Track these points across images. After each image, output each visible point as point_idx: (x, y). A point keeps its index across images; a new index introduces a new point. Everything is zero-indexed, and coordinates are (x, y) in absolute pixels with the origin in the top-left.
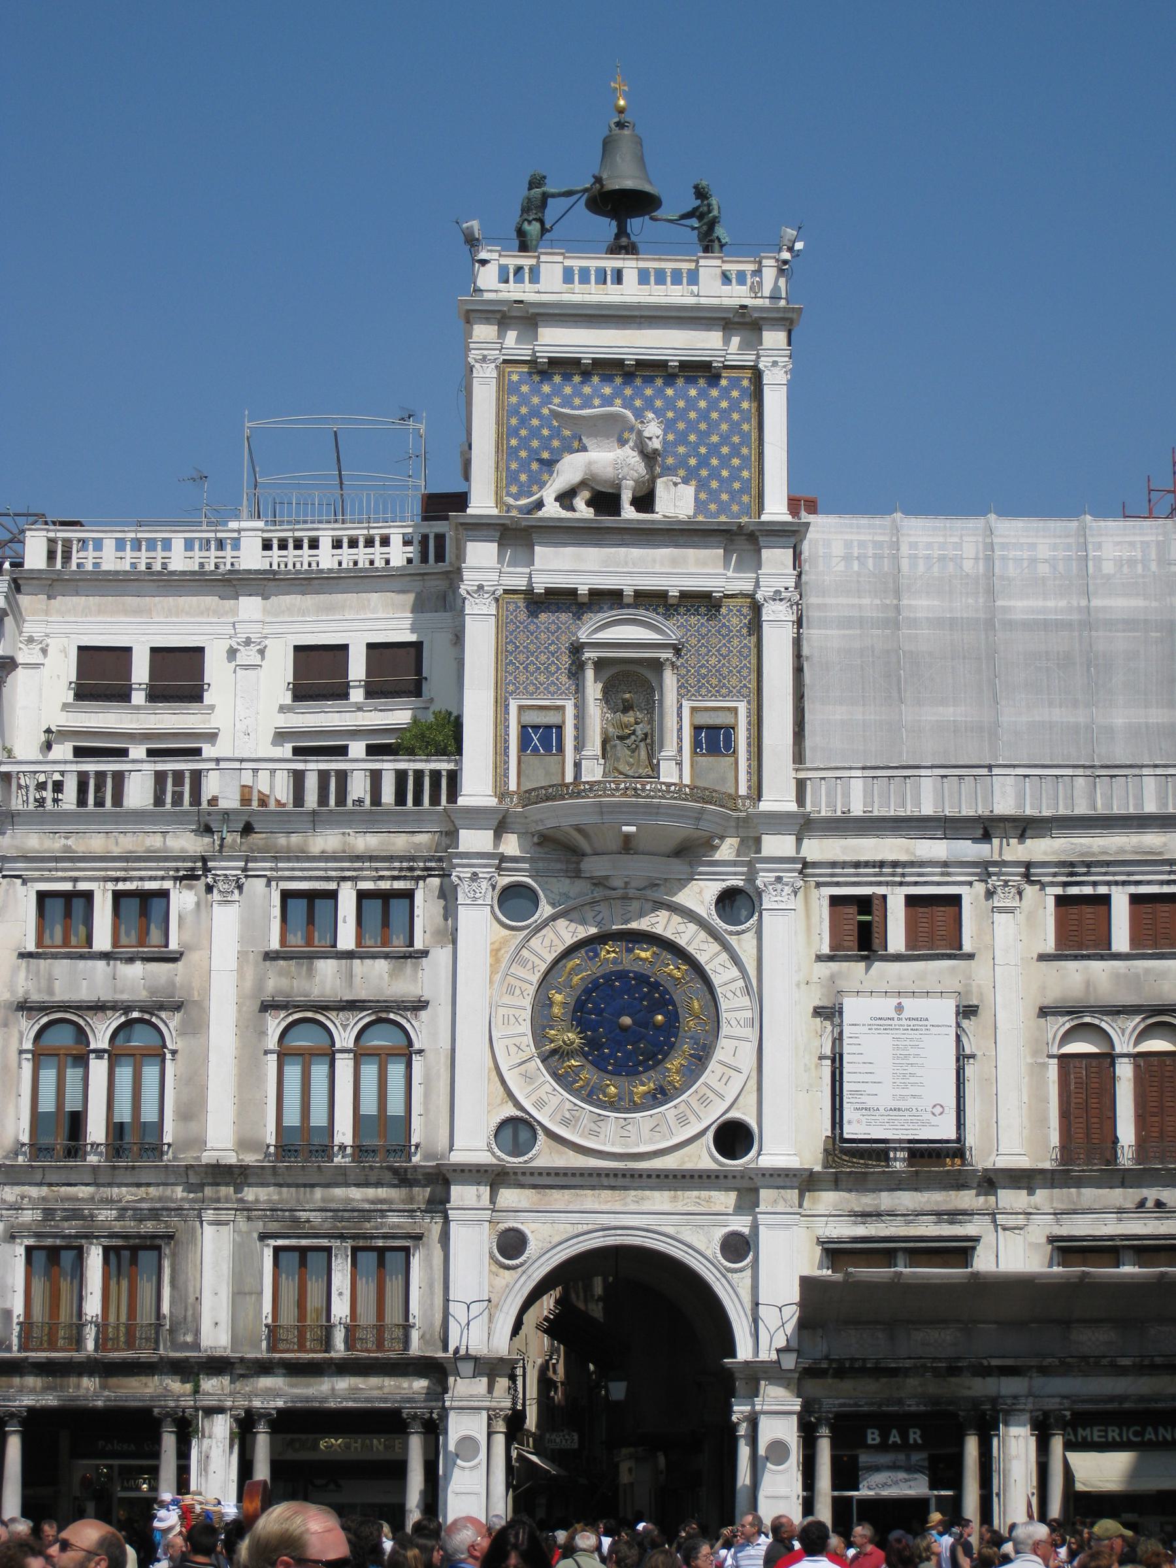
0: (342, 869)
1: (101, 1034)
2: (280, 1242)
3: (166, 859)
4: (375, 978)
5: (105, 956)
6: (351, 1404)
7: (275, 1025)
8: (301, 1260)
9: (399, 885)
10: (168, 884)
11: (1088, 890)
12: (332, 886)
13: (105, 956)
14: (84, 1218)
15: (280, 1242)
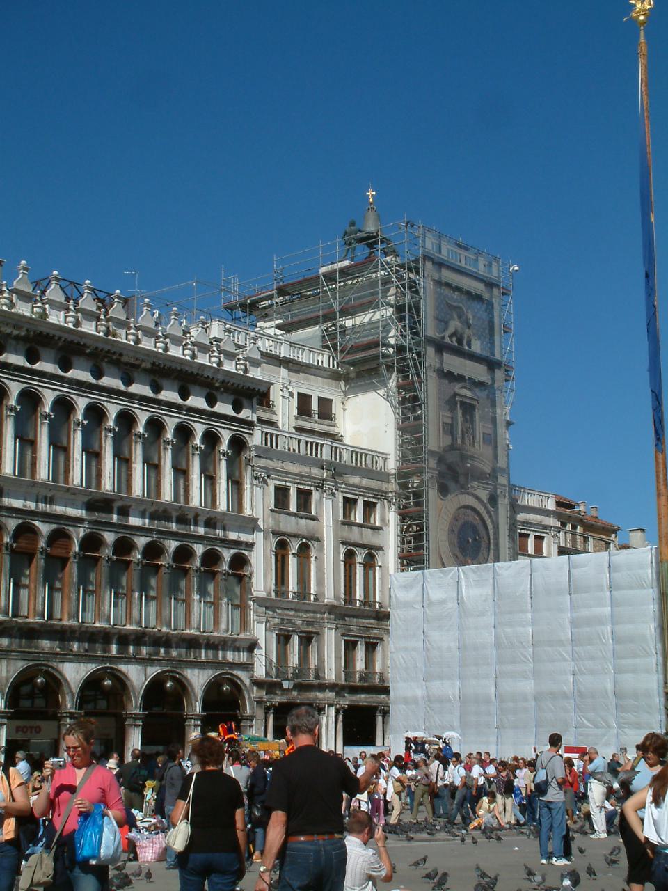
0: (359, 491)
1: (294, 547)
2: (346, 638)
3: (313, 478)
4: (368, 537)
5: (295, 515)
6: (365, 704)
7: (343, 550)
8: (351, 646)
9: (374, 500)
10: (312, 488)
11: (526, 532)
12: (357, 497)
13: (295, 515)
14: (292, 623)
15: (346, 638)
